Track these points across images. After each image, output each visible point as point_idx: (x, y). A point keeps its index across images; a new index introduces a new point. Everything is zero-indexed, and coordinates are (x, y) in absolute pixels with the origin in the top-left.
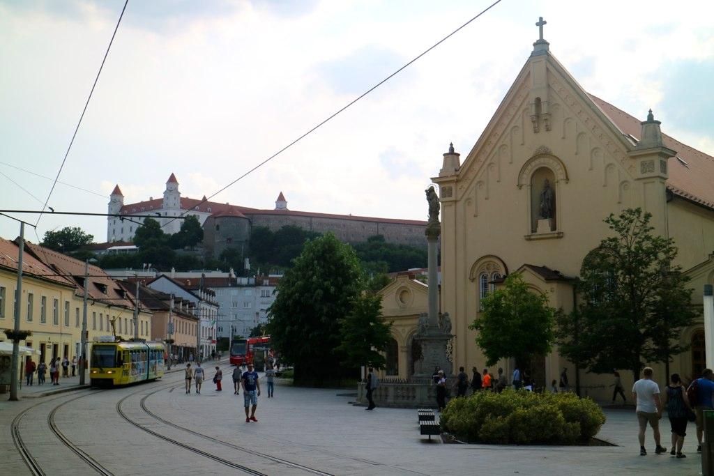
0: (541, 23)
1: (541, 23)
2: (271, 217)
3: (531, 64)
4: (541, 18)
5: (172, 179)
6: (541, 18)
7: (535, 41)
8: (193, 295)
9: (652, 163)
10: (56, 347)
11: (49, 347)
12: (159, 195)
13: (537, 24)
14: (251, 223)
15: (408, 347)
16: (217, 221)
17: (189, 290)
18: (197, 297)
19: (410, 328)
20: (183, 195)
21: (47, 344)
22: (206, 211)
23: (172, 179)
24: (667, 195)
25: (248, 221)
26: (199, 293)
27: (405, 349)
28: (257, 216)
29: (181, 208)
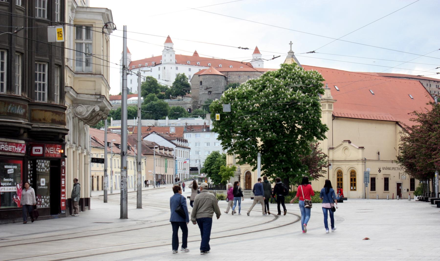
0: (291, 44)
1: (291, 44)
2: (242, 73)
3: (287, 60)
4: (291, 42)
5: (169, 40)
6: (291, 42)
7: (288, 52)
8: (172, 143)
9: (325, 105)
10: (98, 177)
11: (95, 177)
12: (157, 51)
13: (289, 44)
14: (226, 78)
15: (244, 177)
16: (201, 79)
17: (170, 141)
18: (174, 144)
19: (244, 169)
20: (177, 53)
21: (94, 176)
22: (196, 65)
23: (169, 40)
24: (332, 117)
25: (224, 78)
26: (176, 142)
27: (243, 178)
28: (230, 73)
29: (176, 63)
